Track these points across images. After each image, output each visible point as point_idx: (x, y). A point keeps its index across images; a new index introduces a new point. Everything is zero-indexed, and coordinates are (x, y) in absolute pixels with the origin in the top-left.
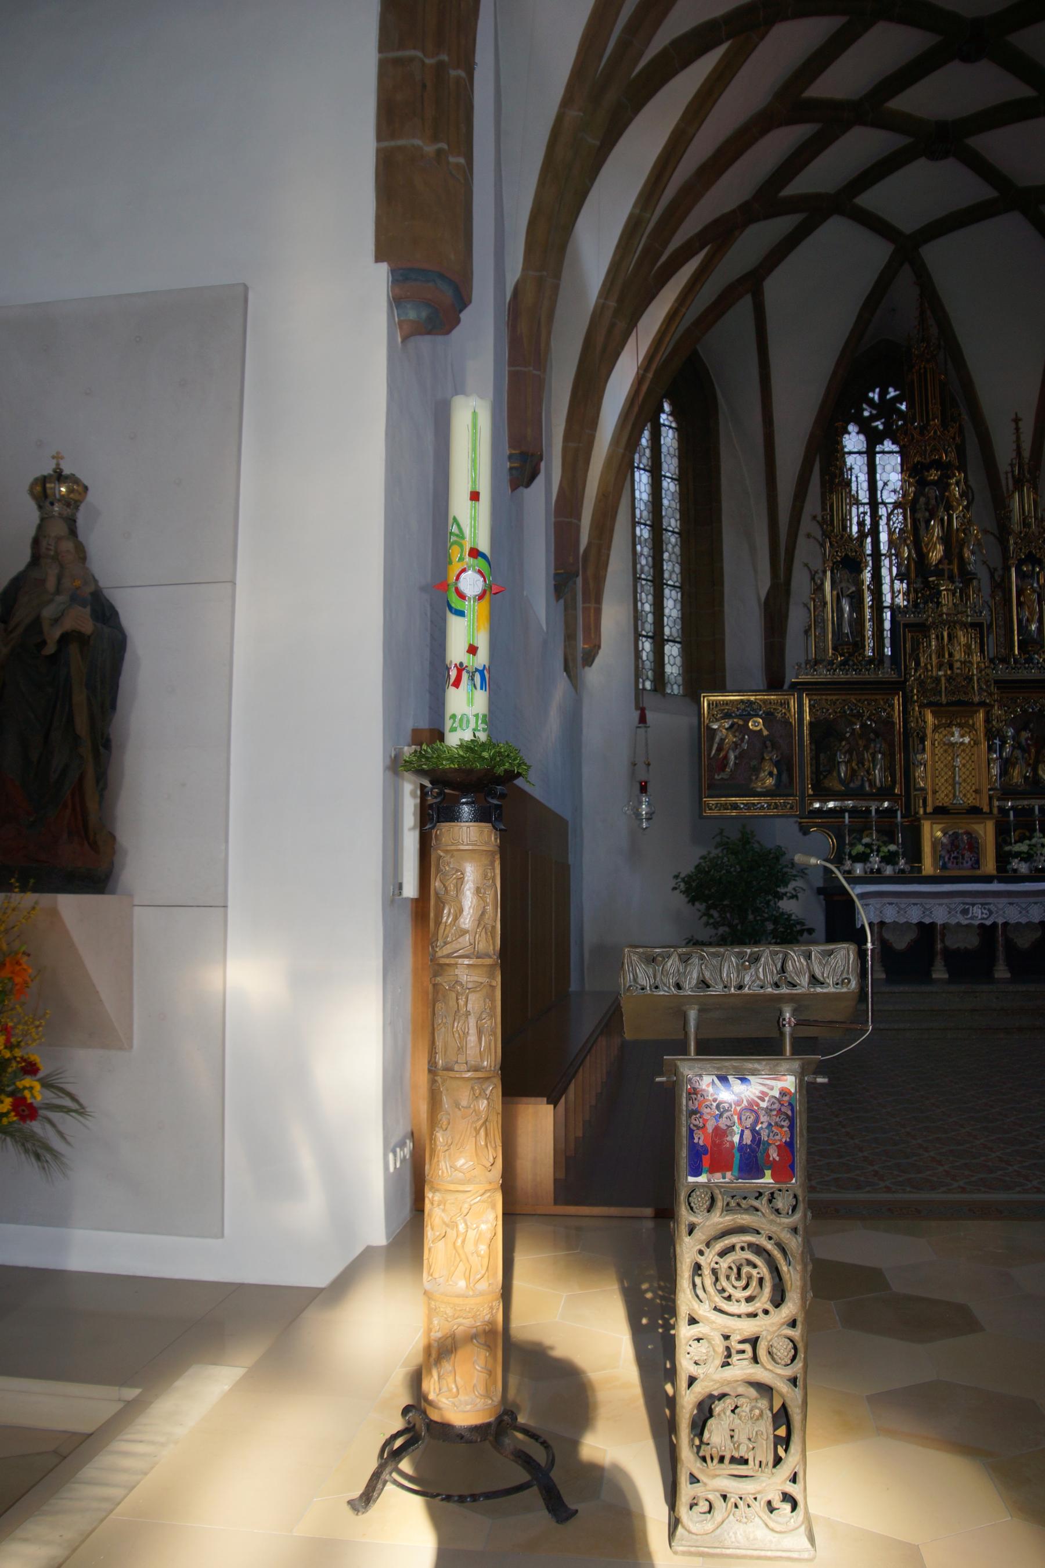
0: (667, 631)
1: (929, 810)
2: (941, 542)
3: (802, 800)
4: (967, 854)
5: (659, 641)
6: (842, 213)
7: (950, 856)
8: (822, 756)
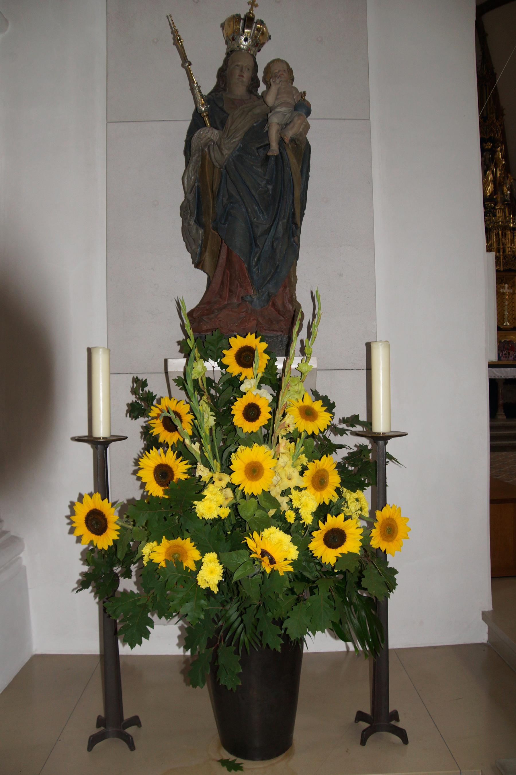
2: (492, 183)
4: (511, 352)
7: (503, 353)
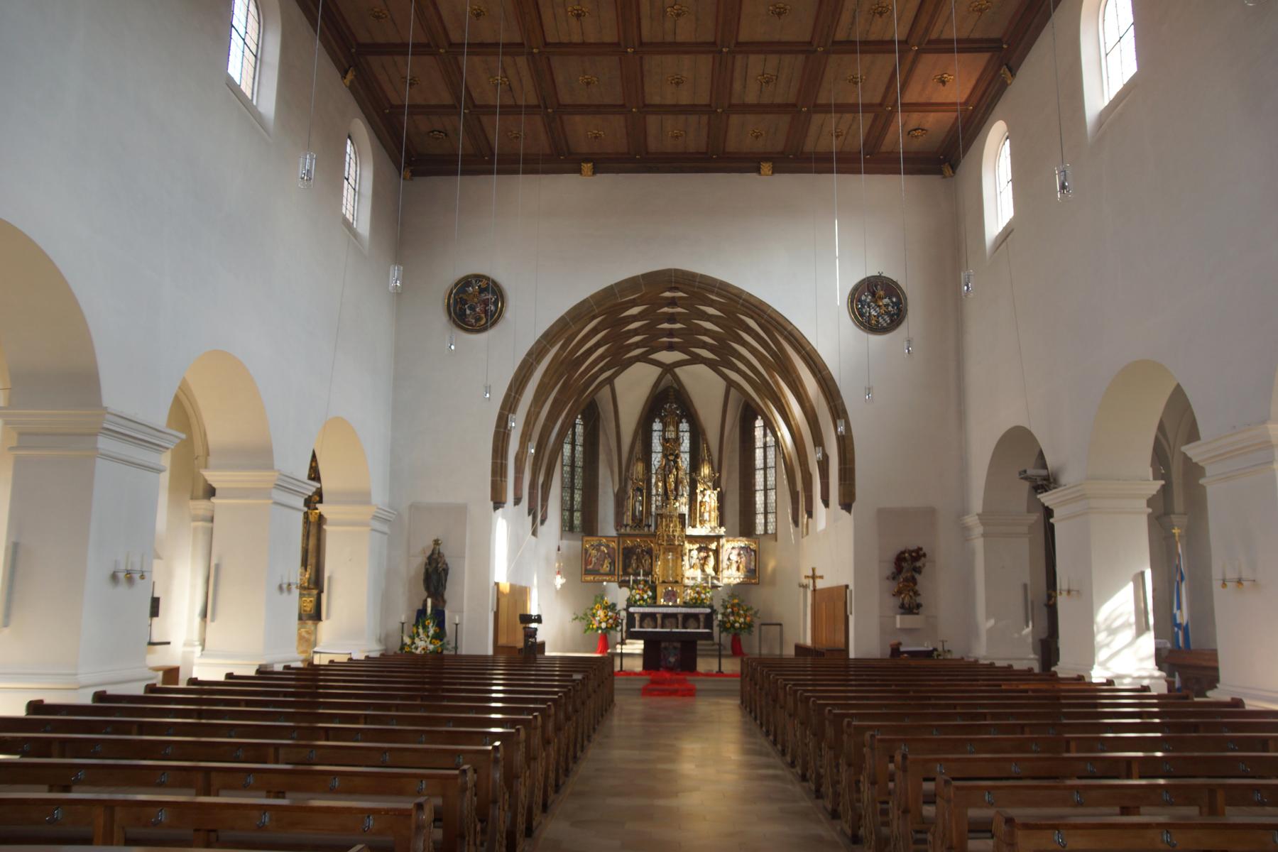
0: (575, 507)
1: (661, 581)
3: (618, 578)
4: (673, 598)
5: (572, 511)
6: (641, 361)
8: (627, 561)
